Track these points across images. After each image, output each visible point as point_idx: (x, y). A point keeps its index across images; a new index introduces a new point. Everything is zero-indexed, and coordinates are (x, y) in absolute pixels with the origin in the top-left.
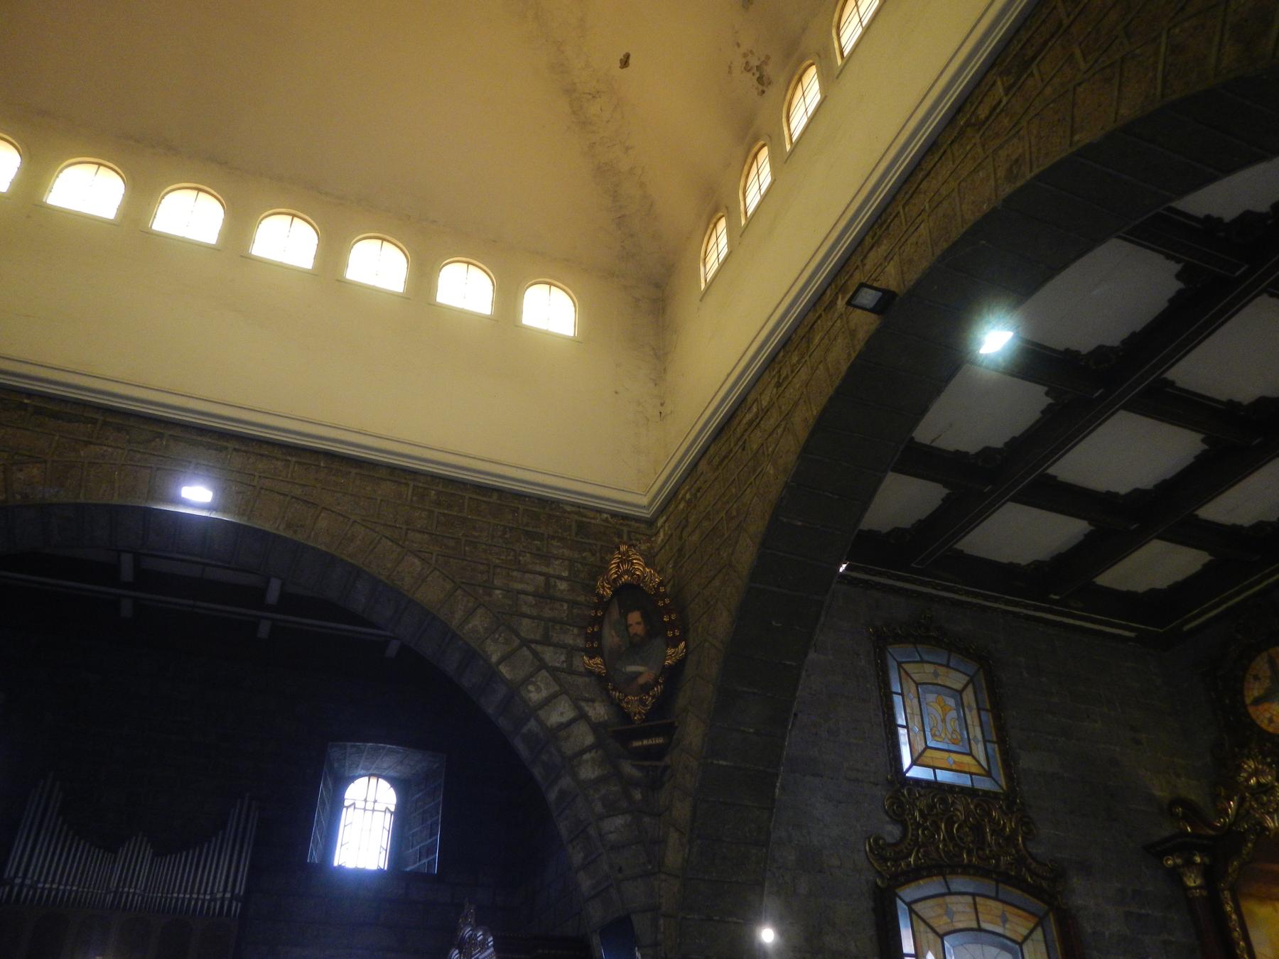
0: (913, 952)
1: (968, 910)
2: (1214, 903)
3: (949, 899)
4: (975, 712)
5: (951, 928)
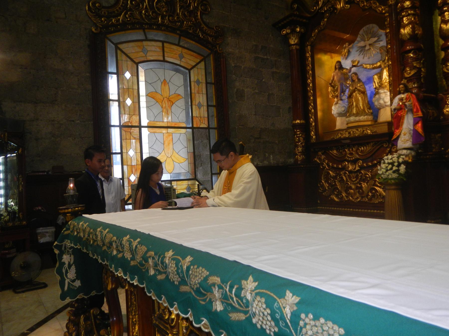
0: (115, 71)
1: (158, 50)
3: (145, 43)
5: (146, 60)
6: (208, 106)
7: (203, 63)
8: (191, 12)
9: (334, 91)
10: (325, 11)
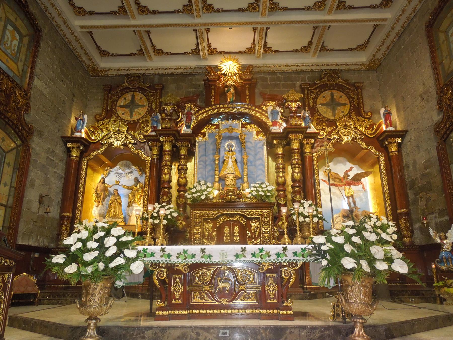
2: (79, 164)
4: (25, 48)
6: (11, 186)
7: (15, 150)
8: (18, 108)
9: (97, 197)
10: (105, 143)
